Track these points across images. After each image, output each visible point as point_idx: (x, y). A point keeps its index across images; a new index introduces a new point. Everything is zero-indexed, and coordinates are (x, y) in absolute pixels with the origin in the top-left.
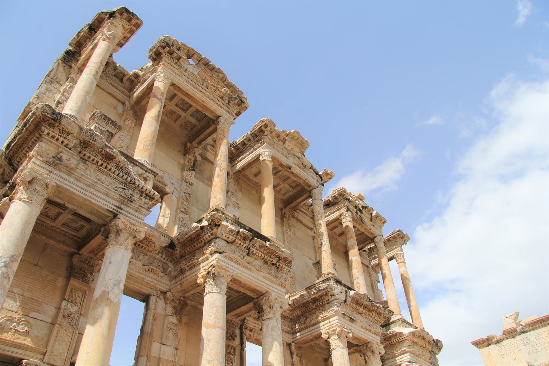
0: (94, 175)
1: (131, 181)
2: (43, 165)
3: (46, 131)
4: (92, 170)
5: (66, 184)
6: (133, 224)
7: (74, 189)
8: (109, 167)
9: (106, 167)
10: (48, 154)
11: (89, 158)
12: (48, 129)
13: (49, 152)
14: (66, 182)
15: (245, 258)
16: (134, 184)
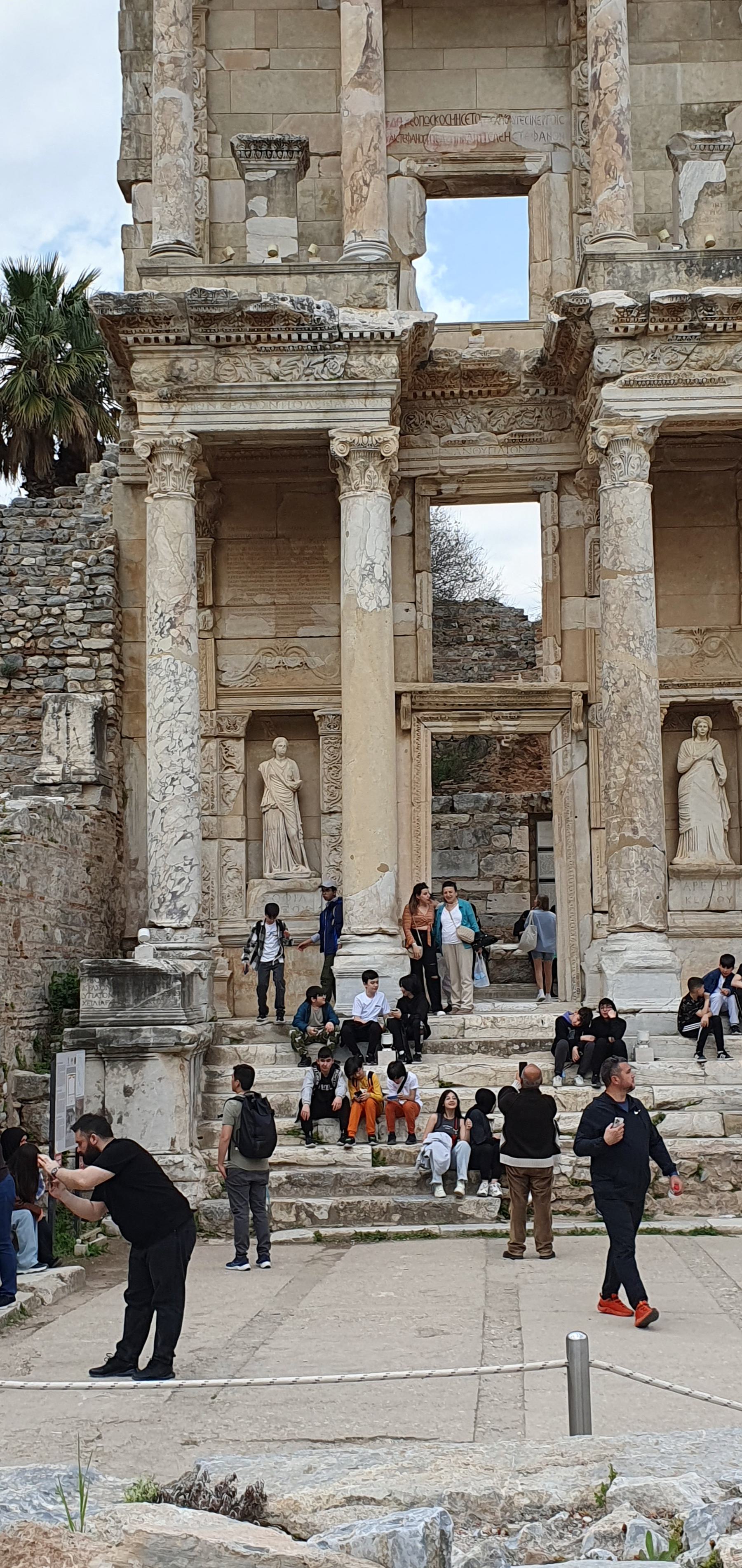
0: (253, 368)
1: (330, 336)
2: (158, 408)
3: (130, 339)
4: (247, 360)
5: (211, 423)
6: (367, 434)
7: (227, 423)
8: (274, 335)
9: (269, 337)
10: (156, 380)
11: (229, 338)
12: (132, 333)
13: (155, 376)
14: (209, 418)
15: (693, 357)
16: (341, 334)
